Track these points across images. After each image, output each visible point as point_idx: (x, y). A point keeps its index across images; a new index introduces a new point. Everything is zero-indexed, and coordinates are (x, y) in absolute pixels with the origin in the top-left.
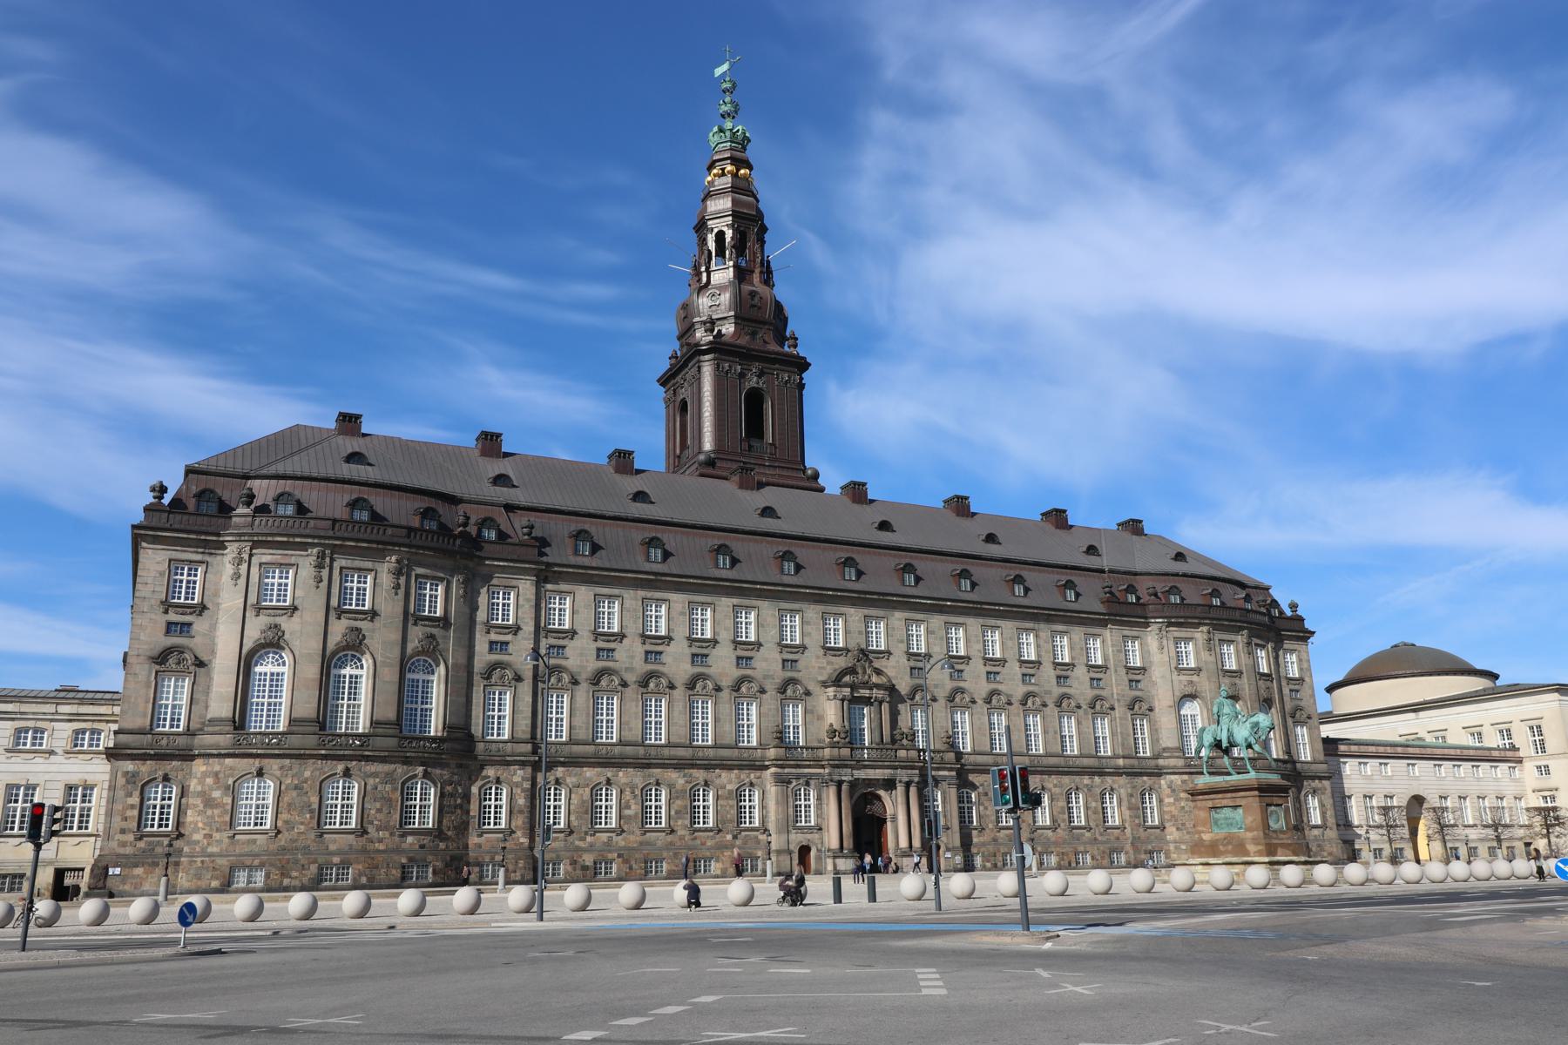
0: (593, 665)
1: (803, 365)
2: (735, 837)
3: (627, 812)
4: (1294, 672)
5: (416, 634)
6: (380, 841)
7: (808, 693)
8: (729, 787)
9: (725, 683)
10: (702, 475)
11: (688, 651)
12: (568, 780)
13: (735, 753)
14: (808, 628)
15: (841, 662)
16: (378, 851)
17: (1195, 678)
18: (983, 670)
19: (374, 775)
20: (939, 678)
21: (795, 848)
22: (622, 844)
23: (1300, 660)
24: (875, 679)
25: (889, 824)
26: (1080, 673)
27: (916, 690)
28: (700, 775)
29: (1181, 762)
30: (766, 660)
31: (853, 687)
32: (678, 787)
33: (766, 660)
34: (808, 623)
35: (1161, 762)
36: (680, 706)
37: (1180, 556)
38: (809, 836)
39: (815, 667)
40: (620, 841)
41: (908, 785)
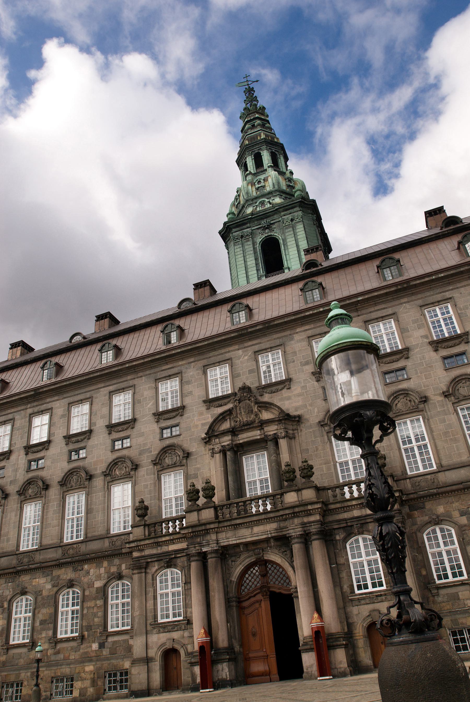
2: (102, 646)
7: (187, 455)
8: (98, 584)
11: (65, 450)
13: (107, 543)
14: (188, 388)
18: (434, 357)
21: (155, 653)
24: (266, 415)
28: (67, 574)
30: (142, 434)
31: (233, 432)
32: (45, 593)
33: (142, 434)
34: (188, 383)
36: (54, 506)
38: (176, 635)
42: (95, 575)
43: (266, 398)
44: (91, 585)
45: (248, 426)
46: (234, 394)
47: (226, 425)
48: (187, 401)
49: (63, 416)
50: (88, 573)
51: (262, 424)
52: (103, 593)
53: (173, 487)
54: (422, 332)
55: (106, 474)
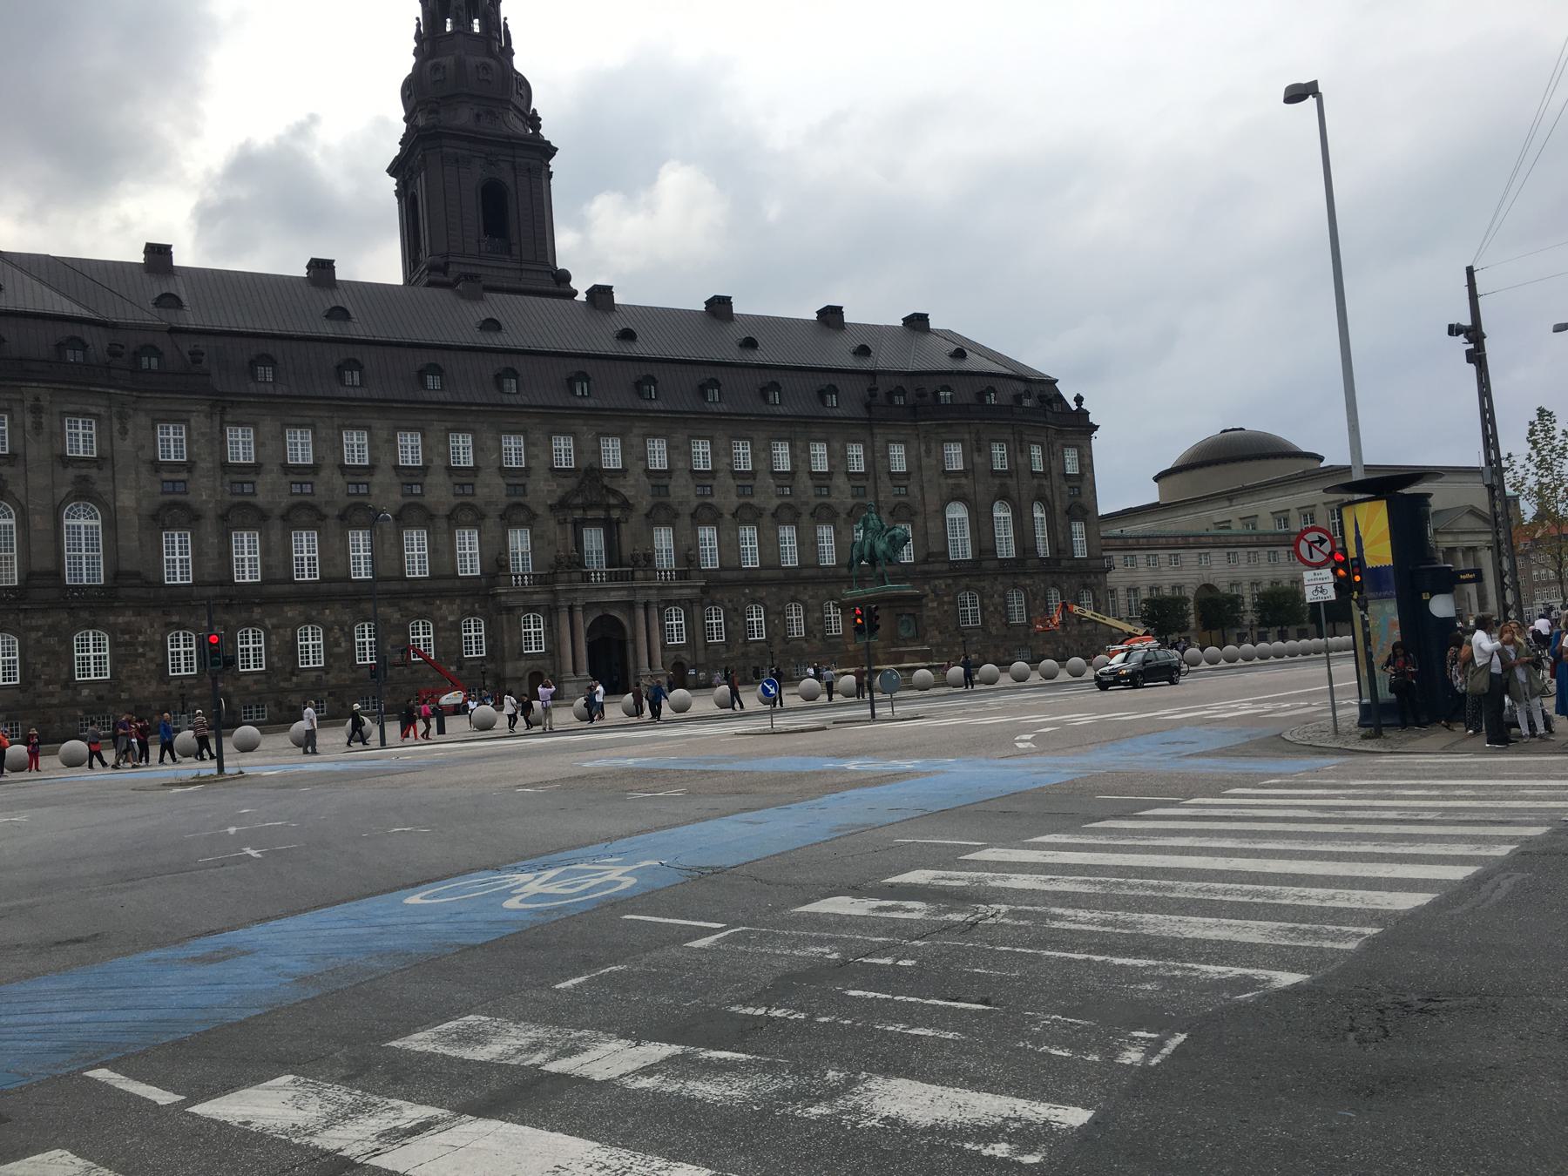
0: (286, 502)
1: (549, 151)
2: (460, 668)
3: (337, 650)
4: (1072, 468)
5: (71, 473)
6: (52, 694)
7: (534, 516)
9: (443, 511)
10: (430, 284)
12: (267, 622)
13: (458, 583)
14: (535, 450)
15: (571, 483)
16: (51, 706)
17: (963, 481)
19: (37, 628)
20: (682, 492)
22: (333, 682)
23: (1081, 457)
25: (630, 647)
26: (840, 481)
27: (656, 507)
29: (946, 567)
30: (488, 486)
33: (488, 486)
34: (534, 445)
35: (926, 567)
37: (960, 354)
38: (540, 663)
39: (543, 491)
40: (331, 679)
41: (647, 606)
42: (448, 611)
43: (606, 481)
44: (444, 619)
45: (597, 506)
46: (576, 470)
47: (579, 500)
48: (533, 464)
49: (388, 441)
50: (440, 608)
51: (608, 507)
52: (456, 627)
53: (519, 541)
54: (728, 460)
55: (449, 517)
